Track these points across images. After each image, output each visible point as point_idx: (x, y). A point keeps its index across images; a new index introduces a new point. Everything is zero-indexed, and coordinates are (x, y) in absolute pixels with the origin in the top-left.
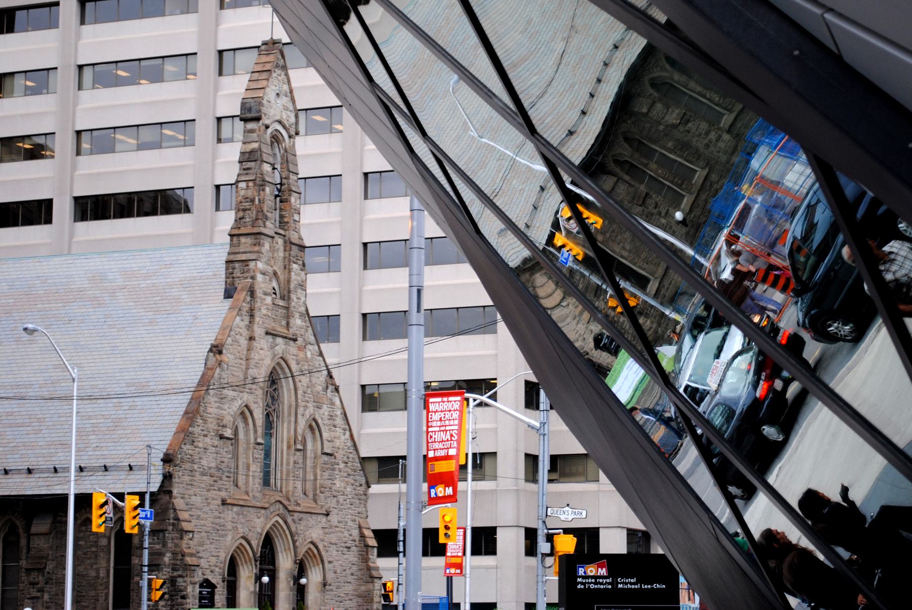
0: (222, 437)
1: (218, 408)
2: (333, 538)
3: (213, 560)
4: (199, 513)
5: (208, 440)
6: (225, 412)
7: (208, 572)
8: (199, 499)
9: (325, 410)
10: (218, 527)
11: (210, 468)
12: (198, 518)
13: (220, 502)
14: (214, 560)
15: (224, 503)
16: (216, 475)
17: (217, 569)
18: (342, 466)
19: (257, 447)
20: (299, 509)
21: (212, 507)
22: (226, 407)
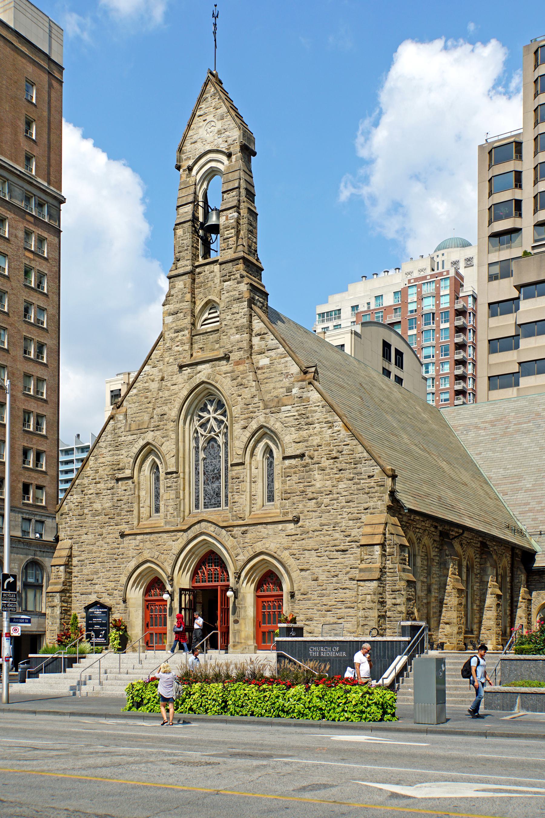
0: (118, 480)
1: (113, 455)
2: (311, 543)
3: (112, 585)
4: (91, 547)
5: (101, 486)
6: (122, 457)
7: (104, 595)
8: (90, 536)
9: (289, 412)
10: (116, 556)
11: (104, 509)
12: (90, 552)
13: (117, 535)
14: (112, 585)
15: (123, 535)
16: (113, 515)
17: (115, 592)
18: (325, 463)
19: (169, 476)
20: (241, 522)
21: (108, 540)
22: (123, 452)
